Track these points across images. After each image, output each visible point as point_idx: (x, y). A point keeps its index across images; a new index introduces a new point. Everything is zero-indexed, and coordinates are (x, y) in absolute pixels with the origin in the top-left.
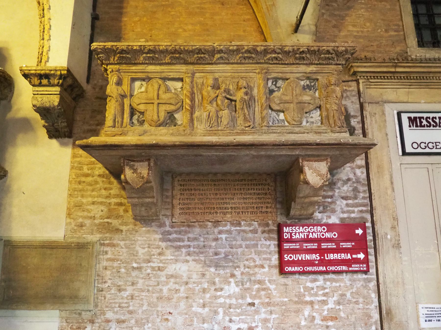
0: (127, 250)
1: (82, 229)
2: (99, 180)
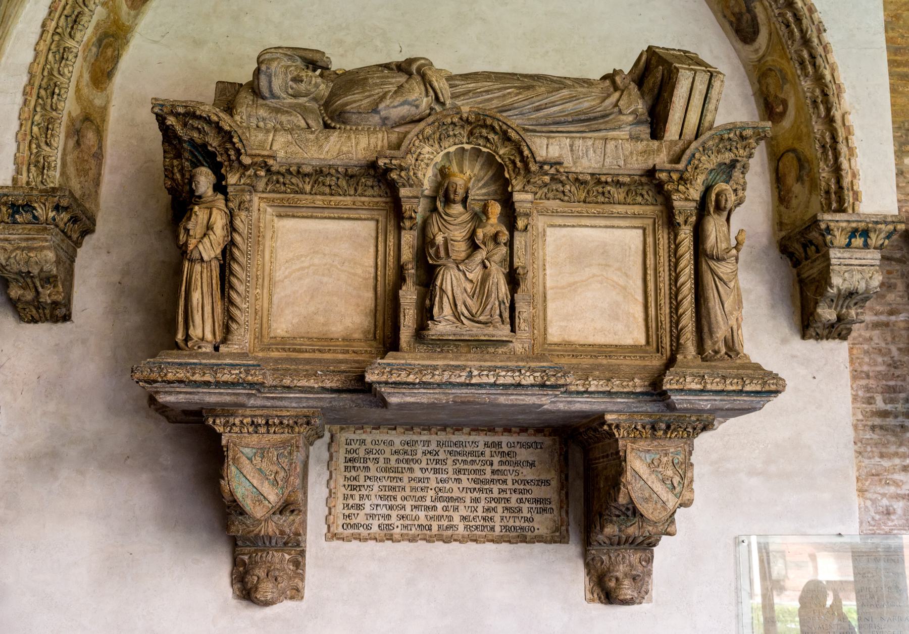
1: (889, 519)
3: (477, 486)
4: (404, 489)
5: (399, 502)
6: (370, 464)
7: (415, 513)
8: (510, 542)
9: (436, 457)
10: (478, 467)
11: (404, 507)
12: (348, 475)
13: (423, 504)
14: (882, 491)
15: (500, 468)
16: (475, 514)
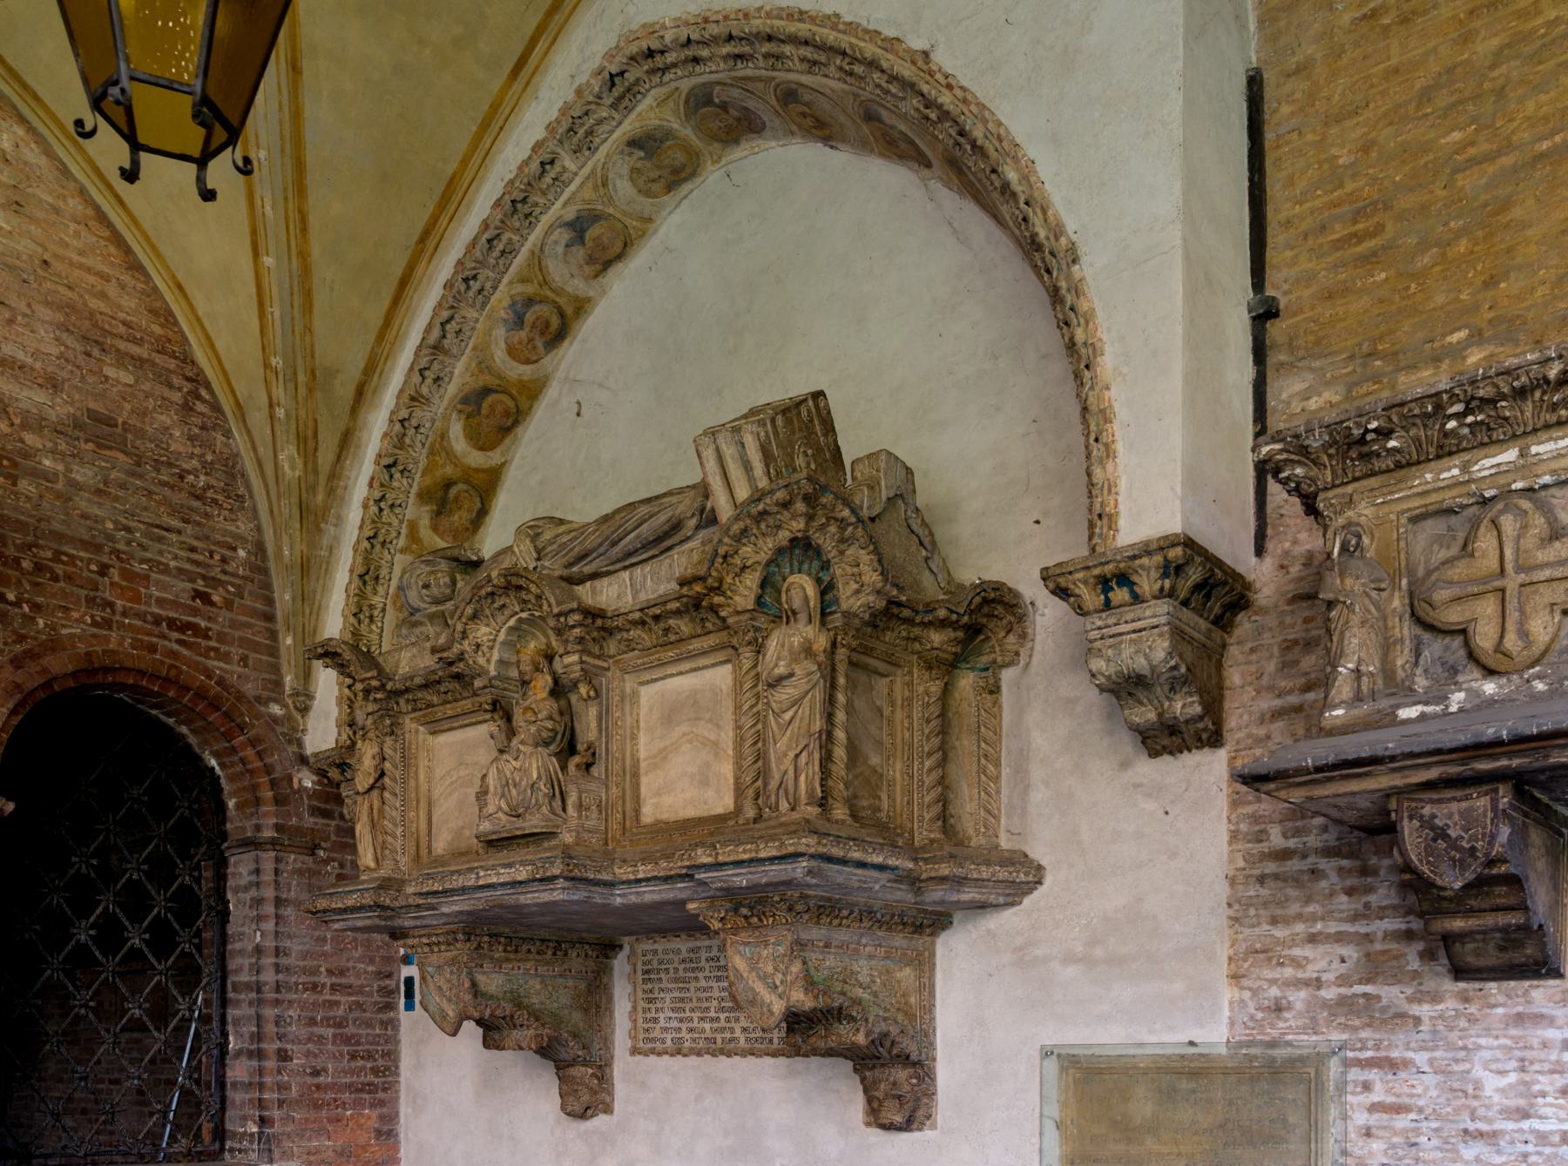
0: (1440, 1078)
1: (1279, 1018)
2: (1324, 864)
14: (1270, 976)
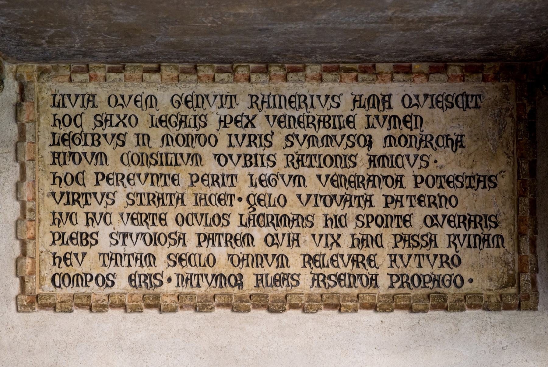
3: (339, 192)
4: (181, 199)
5: (172, 227)
6: (107, 148)
7: (204, 250)
8: (410, 309)
9: (249, 131)
10: (340, 151)
11: (182, 239)
12: (61, 171)
13: (224, 230)
15: (388, 151)
16: (335, 250)
